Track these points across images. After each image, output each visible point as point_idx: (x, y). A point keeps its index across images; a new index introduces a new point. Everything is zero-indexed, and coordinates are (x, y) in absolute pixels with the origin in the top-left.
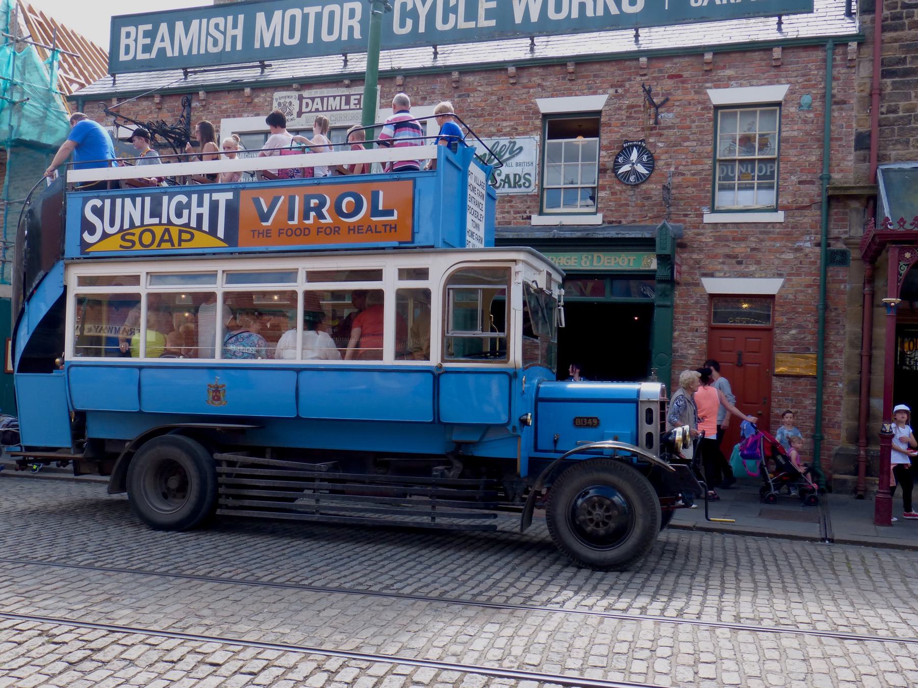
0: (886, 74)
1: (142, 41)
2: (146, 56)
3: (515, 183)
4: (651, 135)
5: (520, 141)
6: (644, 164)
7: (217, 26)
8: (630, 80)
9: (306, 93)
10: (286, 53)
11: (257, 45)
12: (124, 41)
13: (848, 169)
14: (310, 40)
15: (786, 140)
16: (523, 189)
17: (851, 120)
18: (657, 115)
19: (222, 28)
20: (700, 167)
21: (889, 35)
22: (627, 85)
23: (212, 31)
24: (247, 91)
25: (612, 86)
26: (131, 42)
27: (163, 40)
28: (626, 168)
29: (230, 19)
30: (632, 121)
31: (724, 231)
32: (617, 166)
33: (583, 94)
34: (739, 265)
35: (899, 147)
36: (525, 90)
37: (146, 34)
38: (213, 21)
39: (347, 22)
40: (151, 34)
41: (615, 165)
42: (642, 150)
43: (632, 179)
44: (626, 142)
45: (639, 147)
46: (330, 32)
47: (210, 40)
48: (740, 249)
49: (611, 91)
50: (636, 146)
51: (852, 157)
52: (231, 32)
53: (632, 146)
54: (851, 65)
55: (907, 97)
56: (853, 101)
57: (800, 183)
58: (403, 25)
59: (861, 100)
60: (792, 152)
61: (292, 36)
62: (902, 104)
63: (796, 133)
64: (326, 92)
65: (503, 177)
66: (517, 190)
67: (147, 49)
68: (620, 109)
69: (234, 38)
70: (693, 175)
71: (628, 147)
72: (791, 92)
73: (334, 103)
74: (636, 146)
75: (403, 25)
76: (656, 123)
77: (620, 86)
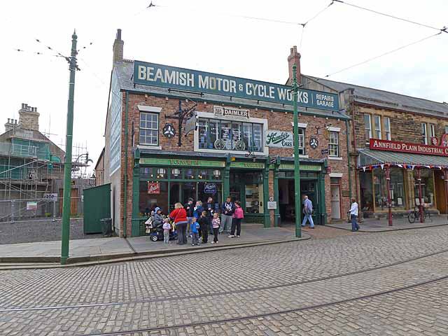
1: (149, 74)
2: (152, 80)
7: (183, 76)
9: (225, 108)
10: (210, 91)
11: (200, 86)
12: (140, 72)
13: (351, 149)
14: (219, 89)
17: (351, 138)
19: (185, 77)
23: (181, 76)
24: (205, 103)
26: (144, 72)
27: (159, 75)
29: (188, 74)
31: (332, 162)
34: (336, 170)
37: (151, 71)
38: (181, 74)
39: (231, 87)
40: (155, 72)
46: (226, 88)
47: (181, 80)
48: (335, 166)
52: (189, 80)
54: (350, 125)
58: (249, 92)
61: (213, 86)
64: (232, 109)
67: (151, 77)
69: (190, 82)
73: (236, 113)
75: (249, 92)
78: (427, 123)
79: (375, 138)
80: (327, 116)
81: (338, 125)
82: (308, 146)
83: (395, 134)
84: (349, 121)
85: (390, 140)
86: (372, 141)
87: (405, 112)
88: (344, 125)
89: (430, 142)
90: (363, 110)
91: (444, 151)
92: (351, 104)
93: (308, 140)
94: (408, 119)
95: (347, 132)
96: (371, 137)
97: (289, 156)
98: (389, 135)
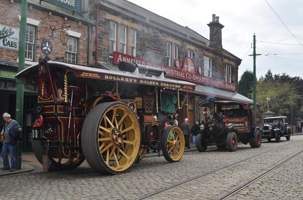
0: (99, 38)
3: (11, 45)
4: (51, 39)
5: (13, 30)
6: (50, 48)
8: (45, 18)
15: (81, 49)
16: (14, 48)
17: (92, 48)
18: (52, 32)
20: (62, 53)
21: (99, 27)
22: (45, 19)
25: (41, 19)
28: (45, 48)
30: (46, 33)
32: (42, 47)
33: (33, 19)
35: (100, 57)
36: (15, 10)
41: (42, 46)
42: (49, 43)
43: (47, 52)
44: (45, 39)
45: (48, 42)
49: (41, 20)
50: (48, 41)
51: (92, 58)
53: (47, 41)
55: (101, 45)
56: (92, 42)
57: (83, 62)
59: (94, 42)
60: (82, 53)
62: (100, 46)
63: (82, 48)
65: (7, 42)
66: (12, 48)
68: (43, 27)
70: (61, 54)
71: (45, 41)
72: (82, 36)
74: (48, 41)
76: (52, 35)
77: (43, 20)
78: (172, 44)
79: (119, 51)
80: (66, 16)
81: (78, 29)
82: (39, 51)
83: (141, 50)
84: (92, 26)
85: (135, 55)
86: (116, 54)
87: (152, 27)
88: (86, 30)
89: (173, 64)
90: (109, 16)
91: (185, 76)
92: (96, 7)
93: (39, 43)
94: (155, 36)
95: (88, 39)
96: (115, 50)
97: (12, 61)
98: (135, 51)
